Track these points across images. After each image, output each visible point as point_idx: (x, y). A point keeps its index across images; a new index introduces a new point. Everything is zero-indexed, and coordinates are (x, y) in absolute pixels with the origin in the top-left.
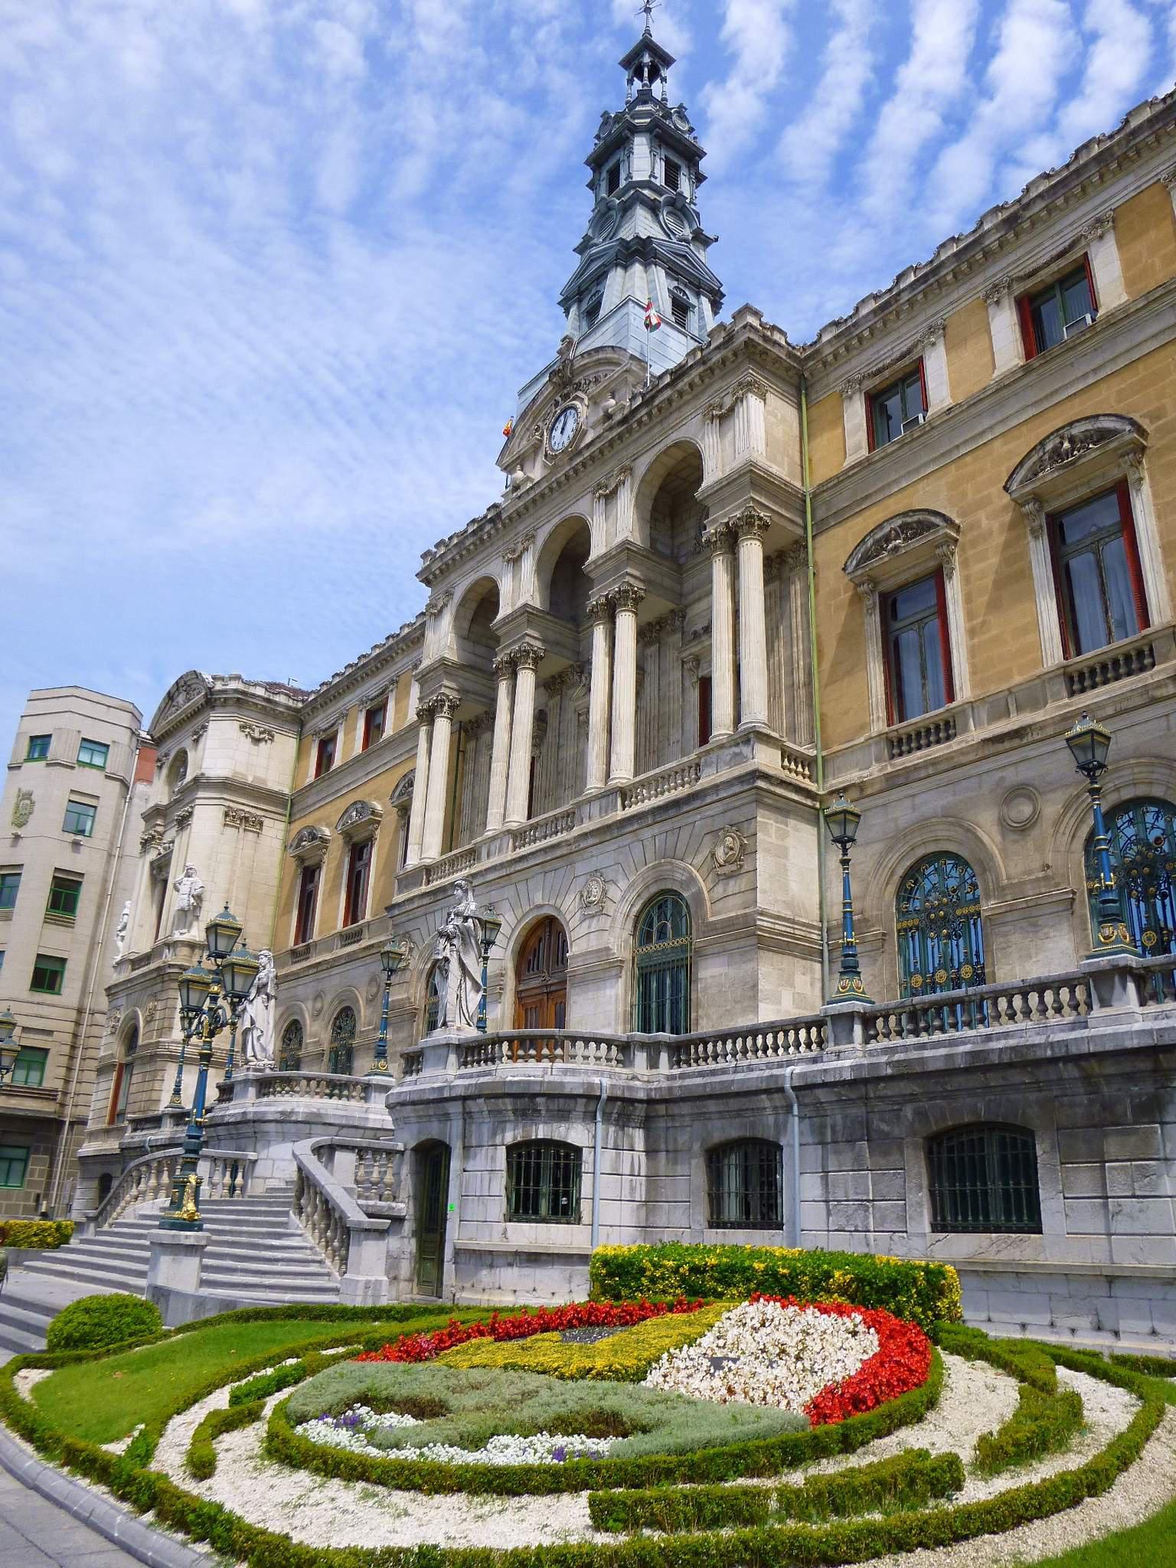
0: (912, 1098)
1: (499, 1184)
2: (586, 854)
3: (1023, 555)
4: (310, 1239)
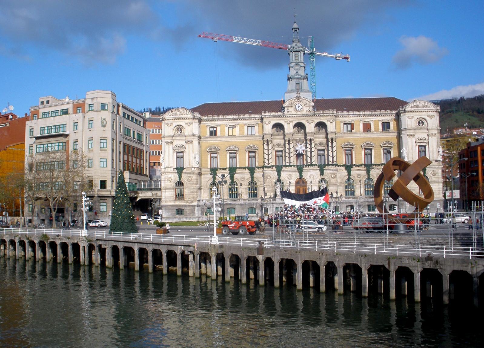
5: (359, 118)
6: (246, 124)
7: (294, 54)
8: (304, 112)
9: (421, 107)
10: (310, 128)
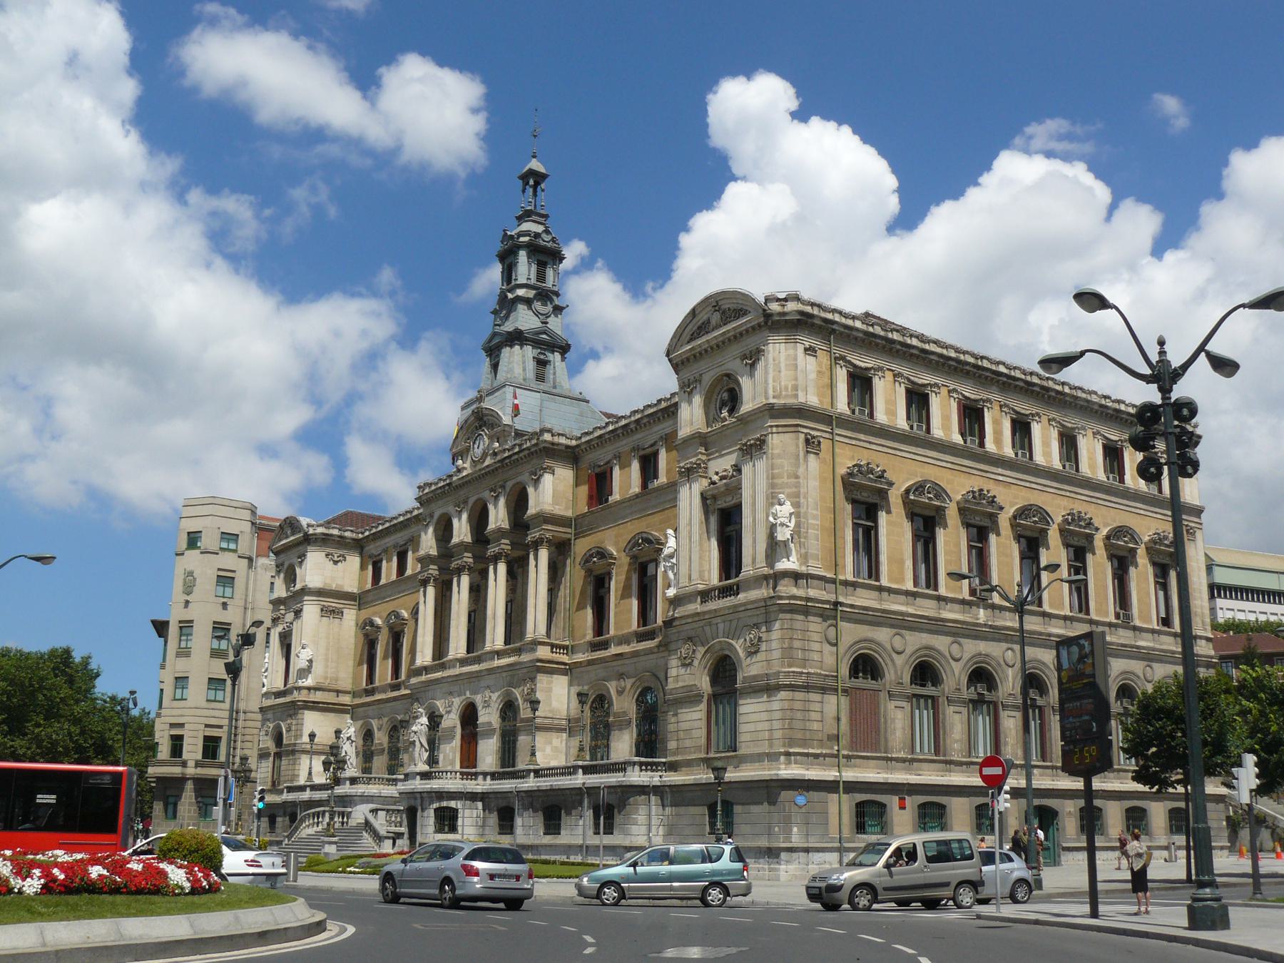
1: (432, 821)
4: (370, 840)
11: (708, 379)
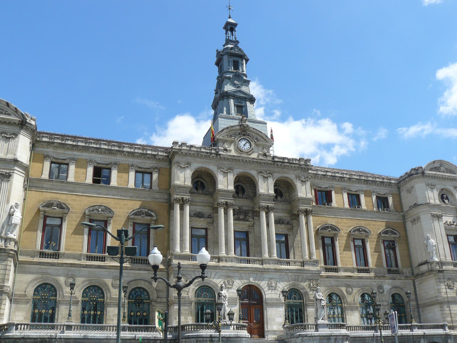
0: (391, 339)
2: (269, 273)
3: (349, 244)
5: (340, 183)
6: (132, 166)
7: (231, 60)
8: (254, 156)
9: (443, 172)
10: (266, 187)
11: (440, 187)
